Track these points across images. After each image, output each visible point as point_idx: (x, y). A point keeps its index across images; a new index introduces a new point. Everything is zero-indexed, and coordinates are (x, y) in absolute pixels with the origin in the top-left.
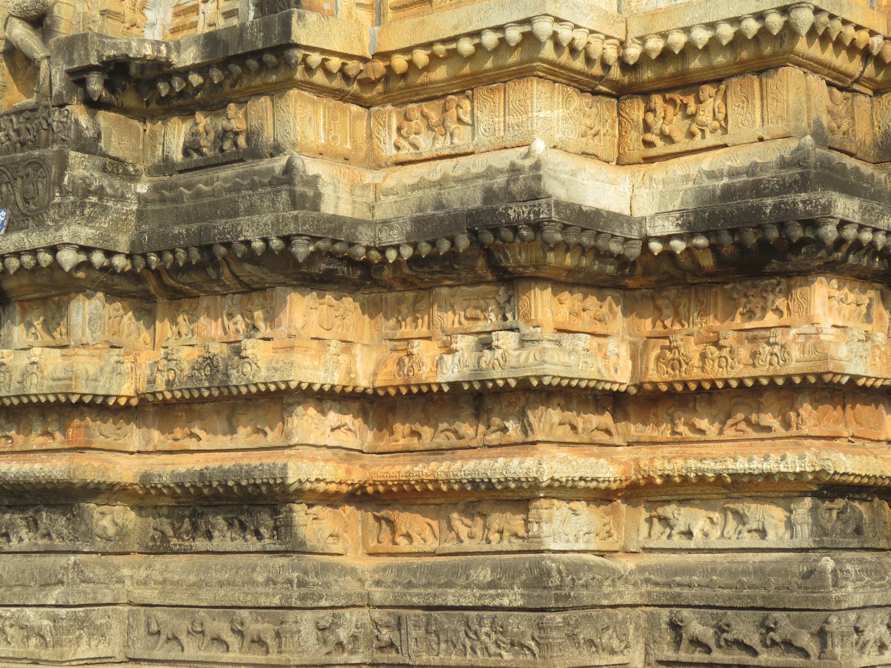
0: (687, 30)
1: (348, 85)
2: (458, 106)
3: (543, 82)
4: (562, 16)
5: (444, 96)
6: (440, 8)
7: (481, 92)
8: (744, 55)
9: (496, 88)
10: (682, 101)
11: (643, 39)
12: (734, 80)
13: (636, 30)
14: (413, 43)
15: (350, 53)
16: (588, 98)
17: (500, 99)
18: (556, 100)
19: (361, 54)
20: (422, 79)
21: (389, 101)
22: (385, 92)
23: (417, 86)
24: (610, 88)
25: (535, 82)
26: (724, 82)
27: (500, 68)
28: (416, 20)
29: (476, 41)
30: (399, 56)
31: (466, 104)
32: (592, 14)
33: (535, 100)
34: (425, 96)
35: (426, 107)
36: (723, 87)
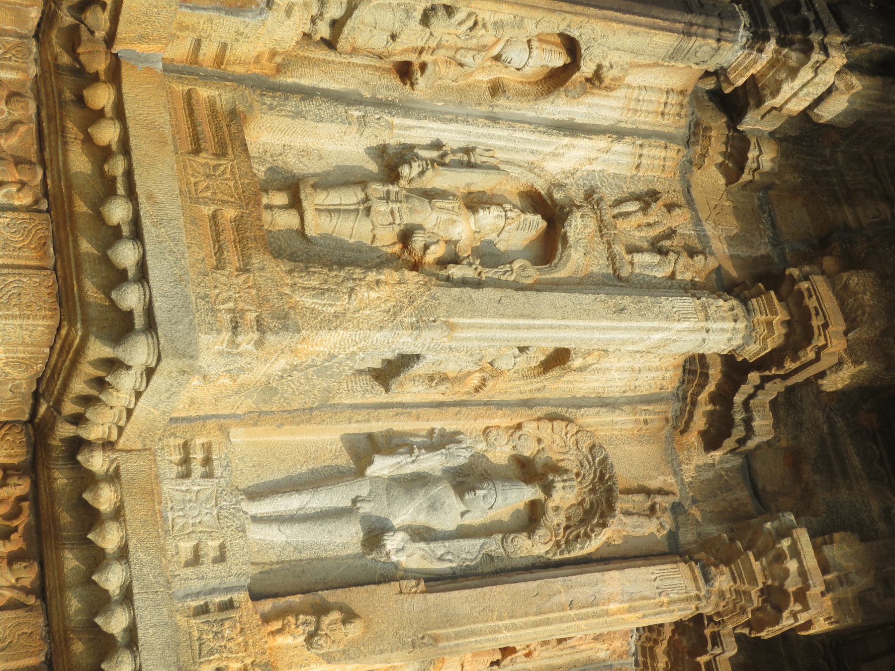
0: (123, 554)
1: (70, 8)
2: (23, 185)
3: (50, 333)
4: (155, 379)
5: (43, 163)
6: (185, 167)
7: (41, 226)
8: (78, 647)
9: (46, 253)
10: (15, 529)
11: (114, 477)
12: (41, 621)
13: (129, 466)
14: (130, 123)
15: (121, 18)
16: (27, 388)
17: (27, 258)
18: (21, 348)
19: (119, 36)
20: (73, 130)
21: (43, 71)
22: (57, 66)
23: (61, 119)
24: (44, 417)
25: (49, 323)
26: (38, 603)
27: (78, 265)
28: (168, 131)
29: (126, 230)
30: (112, 98)
31: (25, 199)
32: (157, 413)
33: (17, 322)
34: (46, 131)
35: (25, 131)
36: (31, 600)
